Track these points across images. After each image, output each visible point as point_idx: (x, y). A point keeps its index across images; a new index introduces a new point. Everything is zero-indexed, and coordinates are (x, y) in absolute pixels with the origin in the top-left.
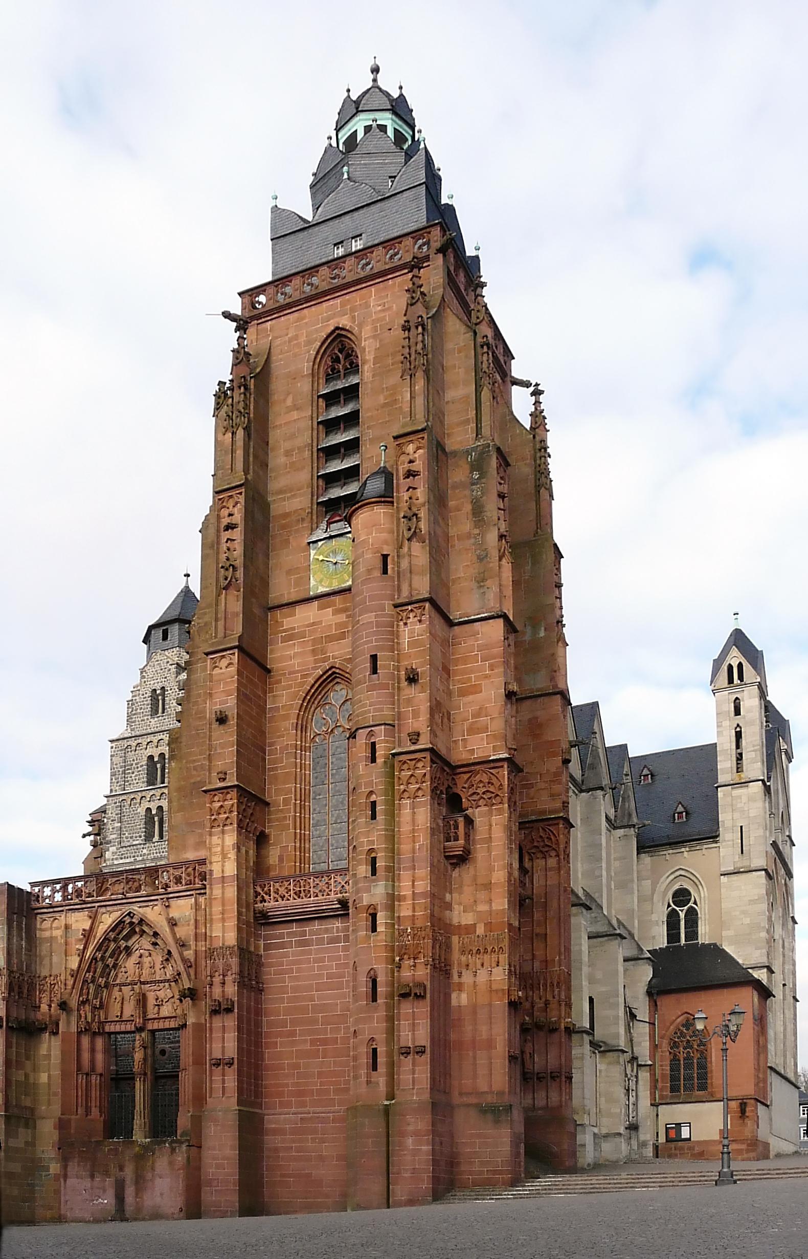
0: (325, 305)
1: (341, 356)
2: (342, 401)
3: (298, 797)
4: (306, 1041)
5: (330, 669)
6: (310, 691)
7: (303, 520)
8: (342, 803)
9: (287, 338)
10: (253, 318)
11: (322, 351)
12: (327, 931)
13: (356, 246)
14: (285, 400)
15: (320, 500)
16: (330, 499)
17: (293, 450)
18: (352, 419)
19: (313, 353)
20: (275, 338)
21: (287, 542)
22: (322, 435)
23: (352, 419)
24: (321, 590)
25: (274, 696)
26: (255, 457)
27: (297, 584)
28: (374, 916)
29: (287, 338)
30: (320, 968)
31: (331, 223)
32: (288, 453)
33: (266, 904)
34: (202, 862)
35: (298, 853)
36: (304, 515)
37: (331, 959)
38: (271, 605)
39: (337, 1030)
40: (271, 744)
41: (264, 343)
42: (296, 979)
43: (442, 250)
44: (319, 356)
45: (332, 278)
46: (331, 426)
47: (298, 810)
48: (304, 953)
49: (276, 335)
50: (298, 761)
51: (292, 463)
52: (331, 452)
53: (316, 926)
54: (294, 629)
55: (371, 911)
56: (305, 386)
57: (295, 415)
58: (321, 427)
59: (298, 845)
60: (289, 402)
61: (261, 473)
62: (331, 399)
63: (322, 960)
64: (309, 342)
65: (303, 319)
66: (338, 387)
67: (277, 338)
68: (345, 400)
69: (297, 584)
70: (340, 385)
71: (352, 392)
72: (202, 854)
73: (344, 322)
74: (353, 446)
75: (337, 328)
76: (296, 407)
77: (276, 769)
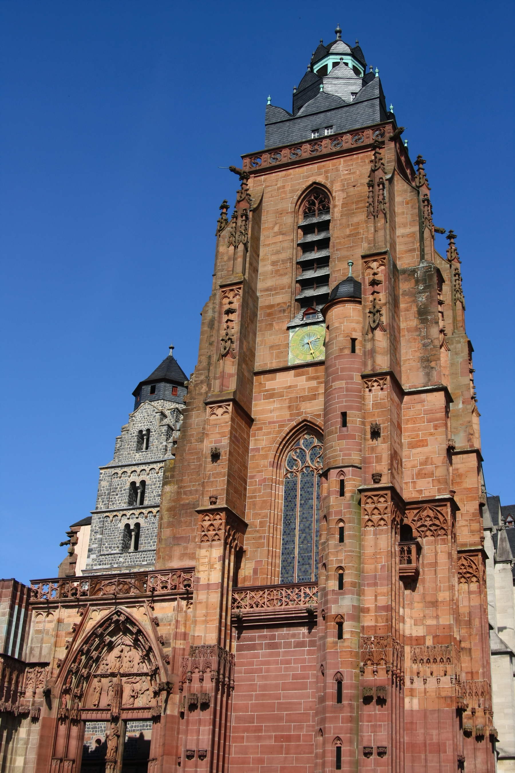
0: (305, 168)
1: (316, 201)
2: (316, 230)
3: (272, 521)
4: (270, 737)
5: (303, 421)
6: (285, 437)
7: (284, 311)
8: (308, 527)
9: (276, 187)
10: (251, 173)
11: (302, 197)
12: (294, 636)
13: (328, 133)
14: (273, 228)
15: (297, 298)
16: (306, 298)
17: (277, 262)
18: (324, 244)
19: (296, 198)
20: (267, 186)
21: (271, 325)
22: (300, 252)
23: (324, 244)
24: (297, 362)
25: (256, 440)
26: (251, 264)
27: (278, 357)
28: (340, 625)
29: (276, 187)
30: (286, 669)
31: (311, 118)
32: (274, 263)
33: (242, 610)
34: (190, 570)
35: (270, 567)
36: (285, 307)
37: (296, 661)
38: (256, 370)
39: (301, 728)
40: (252, 477)
41: (260, 188)
42: (265, 678)
43: (391, 139)
44: (300, 201)
45: (311, 151)
46: (306, 247)
47: (271, 531)
48: (271, 655)
49: (268, 184)
50: (273, 492)
51: (277, 271)
52: (306, 265)
53: (285, 631)
54: (274, 389)
55: (338, 620)
56: (289, 220)
57: (280, 238)
58: (299, 248)
59: (270, 560)
60: (276, 229)
61: (253, 275)
62: (307, 229)
63: (288, 662)
64: (293, 191)
65: (290, 175)
66: (313, 222)
67: (268, 186)
68: (318, 232)
69: (278, 357)
70: (315, 220)
71: (324, 226)
72: (188, 563)
73: (320, 179)
74: (324, 262)
75: (314, 183)
76: (281, 233)
77: (255, 497)
